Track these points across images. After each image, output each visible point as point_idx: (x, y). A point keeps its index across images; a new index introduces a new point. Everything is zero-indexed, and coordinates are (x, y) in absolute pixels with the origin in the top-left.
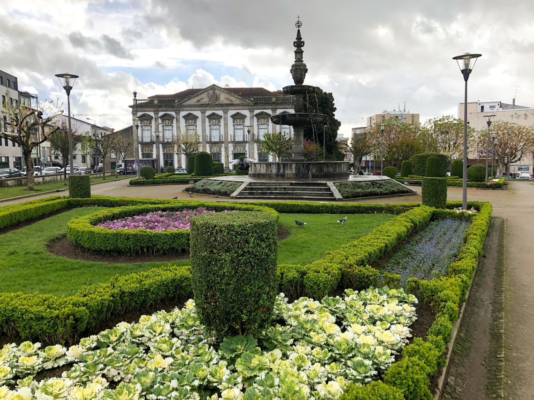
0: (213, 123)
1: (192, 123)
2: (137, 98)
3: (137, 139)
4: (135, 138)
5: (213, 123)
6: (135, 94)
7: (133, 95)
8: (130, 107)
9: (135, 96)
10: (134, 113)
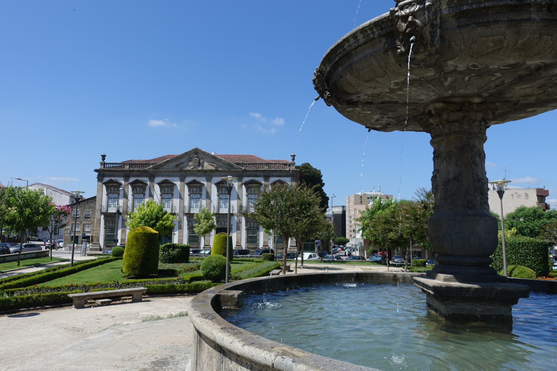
0: (193, 191)
1: (168, 190)
2: (106, 161)
3: (100, 208)
4: (98, 207)
5: (193, 191)
6: (104, 157)
7: (101, 157)
8: (96, 171)
9: (103, 159)
10: (100, 179)
